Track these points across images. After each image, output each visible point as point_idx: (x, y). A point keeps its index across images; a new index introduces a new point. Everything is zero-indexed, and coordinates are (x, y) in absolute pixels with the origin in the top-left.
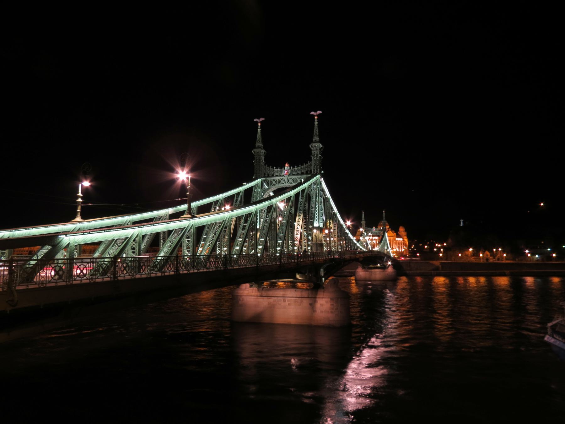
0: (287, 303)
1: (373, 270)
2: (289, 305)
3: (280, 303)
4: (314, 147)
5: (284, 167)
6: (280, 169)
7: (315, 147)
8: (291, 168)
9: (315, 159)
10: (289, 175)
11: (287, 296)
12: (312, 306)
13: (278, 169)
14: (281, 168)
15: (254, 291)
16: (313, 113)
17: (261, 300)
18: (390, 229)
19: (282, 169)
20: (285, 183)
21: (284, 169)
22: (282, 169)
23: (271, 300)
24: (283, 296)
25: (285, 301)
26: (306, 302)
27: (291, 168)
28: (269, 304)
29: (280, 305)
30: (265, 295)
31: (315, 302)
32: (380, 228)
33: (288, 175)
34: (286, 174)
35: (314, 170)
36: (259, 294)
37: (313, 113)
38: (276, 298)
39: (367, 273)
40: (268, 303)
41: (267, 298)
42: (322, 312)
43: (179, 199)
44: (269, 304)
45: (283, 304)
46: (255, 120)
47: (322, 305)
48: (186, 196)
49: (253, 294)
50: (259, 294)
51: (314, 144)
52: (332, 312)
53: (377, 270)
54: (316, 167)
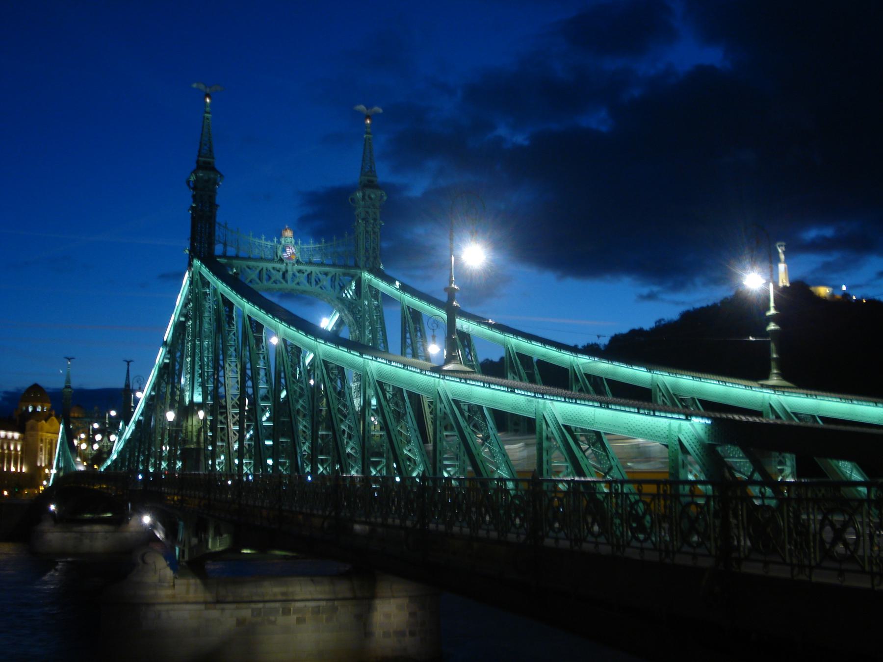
0: (293, 618)
1: (86, 528)
2: (300, 621)
3: (272, 618)
4: (367, 198)
5: (280, 236)
6: (266, 240)
7: (370, 198)
8: (299, 242)
9: (369, 229)
10: (298, 262)
11: (297, 597)
12: (363, 620)
13: (260, 238)
14: (269, 238)
15: (192, 589)
16: (361, 108)
17: (214, 613)
18: (53, 413)
19: (272, 241)
20: (287, 282)
21: (279, 242)
22: (272, 241)
23: (246, 612)
24: (284, 598)
25: (286, 612)
26: (345, 614)
27: (299, 242)
28: (240, 622)
29: (274, 623)
30: (230, 599)
31: (370, 609)
32: (27, 409)
33: (295, 262)
34: (289, 258)
35: (368, 258)
36: (209, 597)
37: (361, 108)
38: (260, 605)
39: (68, 535)
40: (238, 620)
41: (233, 606)
42: (386, 635)
43: (751, 339)
44: (240, 622)
45: (281, 620)
46: (195, 85)
47: (387, 616)
48: (764, 333)
49: (191, 596)
50: (209, 597)
51: (368, 191)
52: (412, 634)
53: (97, 528)
54: (371, 252)
